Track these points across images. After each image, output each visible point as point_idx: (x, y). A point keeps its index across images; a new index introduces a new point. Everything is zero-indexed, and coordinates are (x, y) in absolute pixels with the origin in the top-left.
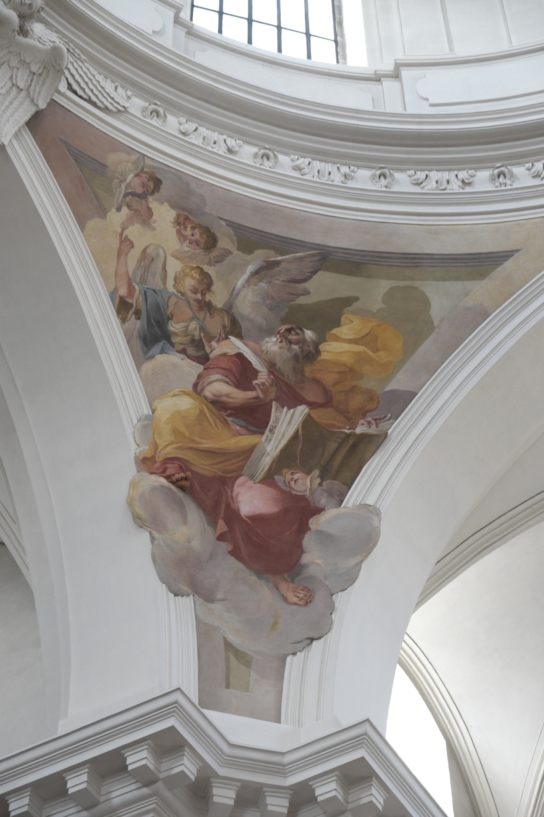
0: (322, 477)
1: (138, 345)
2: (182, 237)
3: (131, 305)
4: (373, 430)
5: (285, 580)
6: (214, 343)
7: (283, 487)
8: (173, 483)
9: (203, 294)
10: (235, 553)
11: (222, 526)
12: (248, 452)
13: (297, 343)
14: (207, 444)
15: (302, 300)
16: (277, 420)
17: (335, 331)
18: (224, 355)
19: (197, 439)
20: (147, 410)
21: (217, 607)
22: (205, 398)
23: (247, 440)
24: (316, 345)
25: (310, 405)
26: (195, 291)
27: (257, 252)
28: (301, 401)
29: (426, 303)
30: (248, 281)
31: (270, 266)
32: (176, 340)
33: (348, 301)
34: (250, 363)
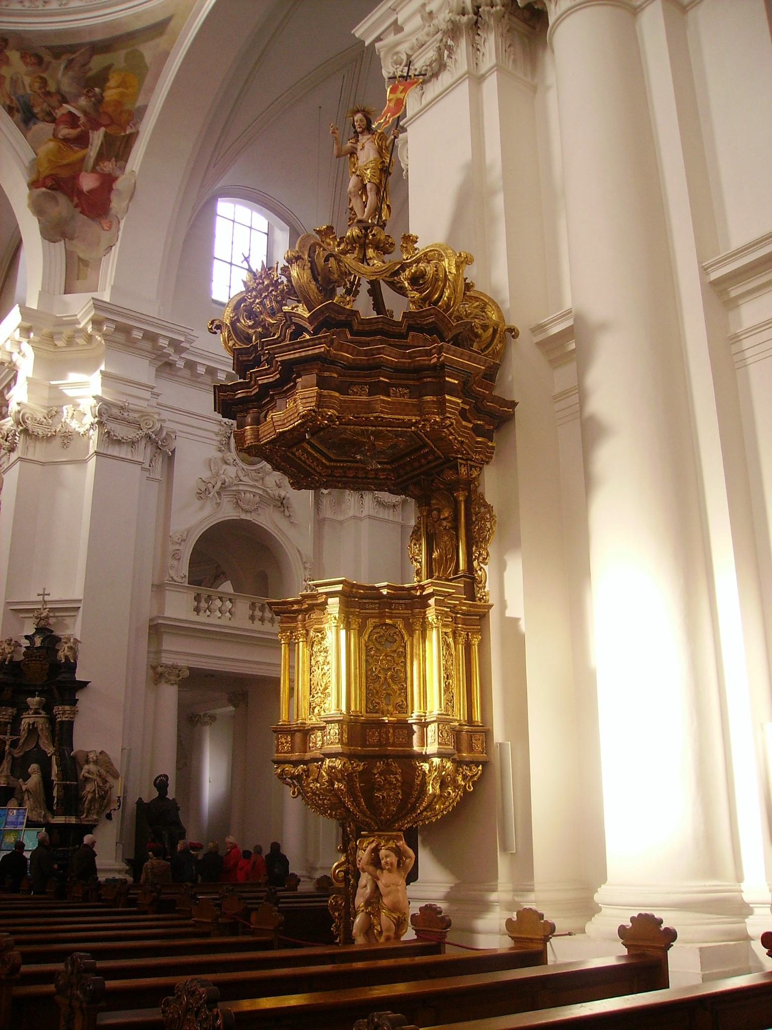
0: (116, 161)
1: (22, 125)
2: (26, 64)
3: (13, 107)
4: (133, 130)
5: (103, 218)
6: (57, 111)
7: (100, 171)
8: (49, 189)
9: (45, 88)
10: (82, 212)
11: (76, 200)
12: (83, 159)
13: (93, 97)
14: (65, 162)
15: (91, 74)
16: (93, 138)
17: (108, 84)
18: (63, 115)
19: (59, 161)
20: (33, 155)
21: (75, 242)
22: (60, 139)
23: (80, 154)
24: (101, 94)
25: (106, 126)
26: (40, 88)
27: (63, 57)
28: (102, 125)
29: (142, 56)
30: (63, 74)
31: (70, 62)
32: (39, 116)
33: (110, 67)
34: (75, 114)
